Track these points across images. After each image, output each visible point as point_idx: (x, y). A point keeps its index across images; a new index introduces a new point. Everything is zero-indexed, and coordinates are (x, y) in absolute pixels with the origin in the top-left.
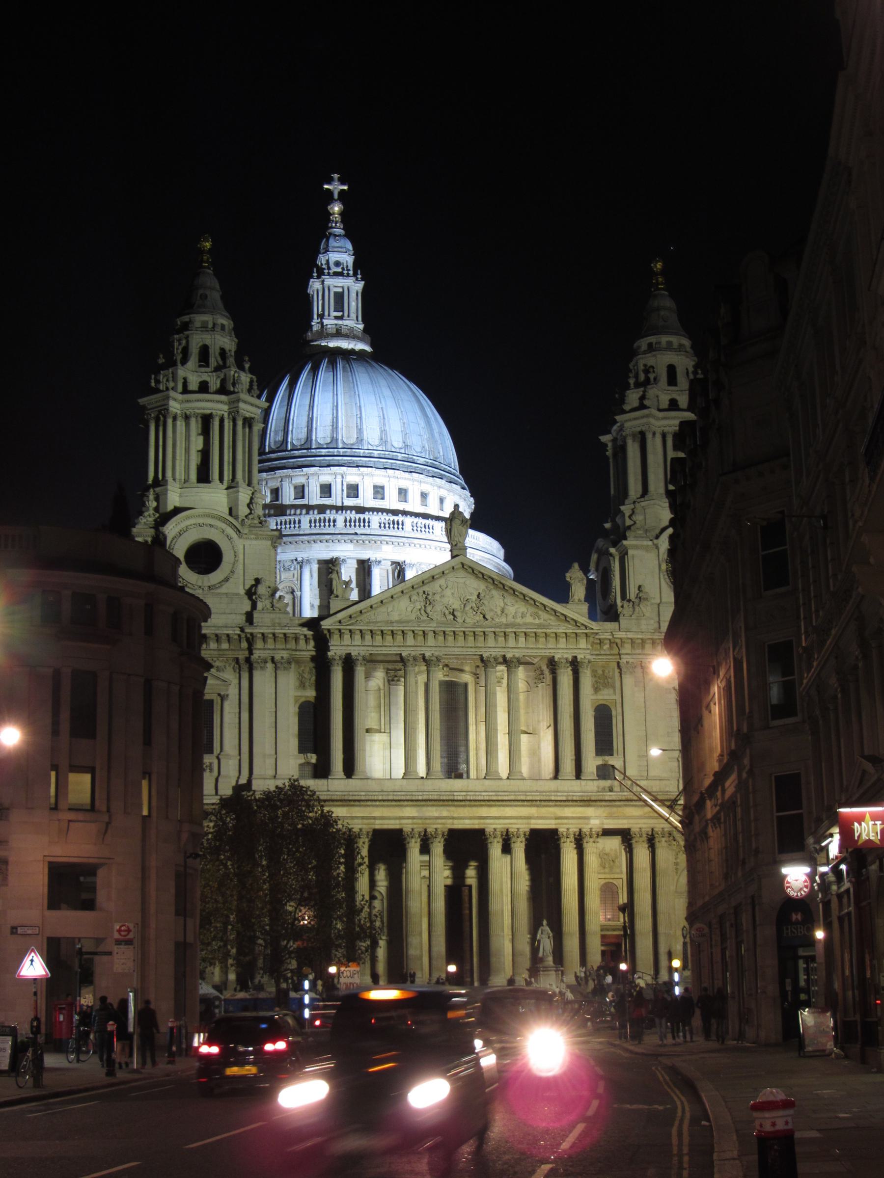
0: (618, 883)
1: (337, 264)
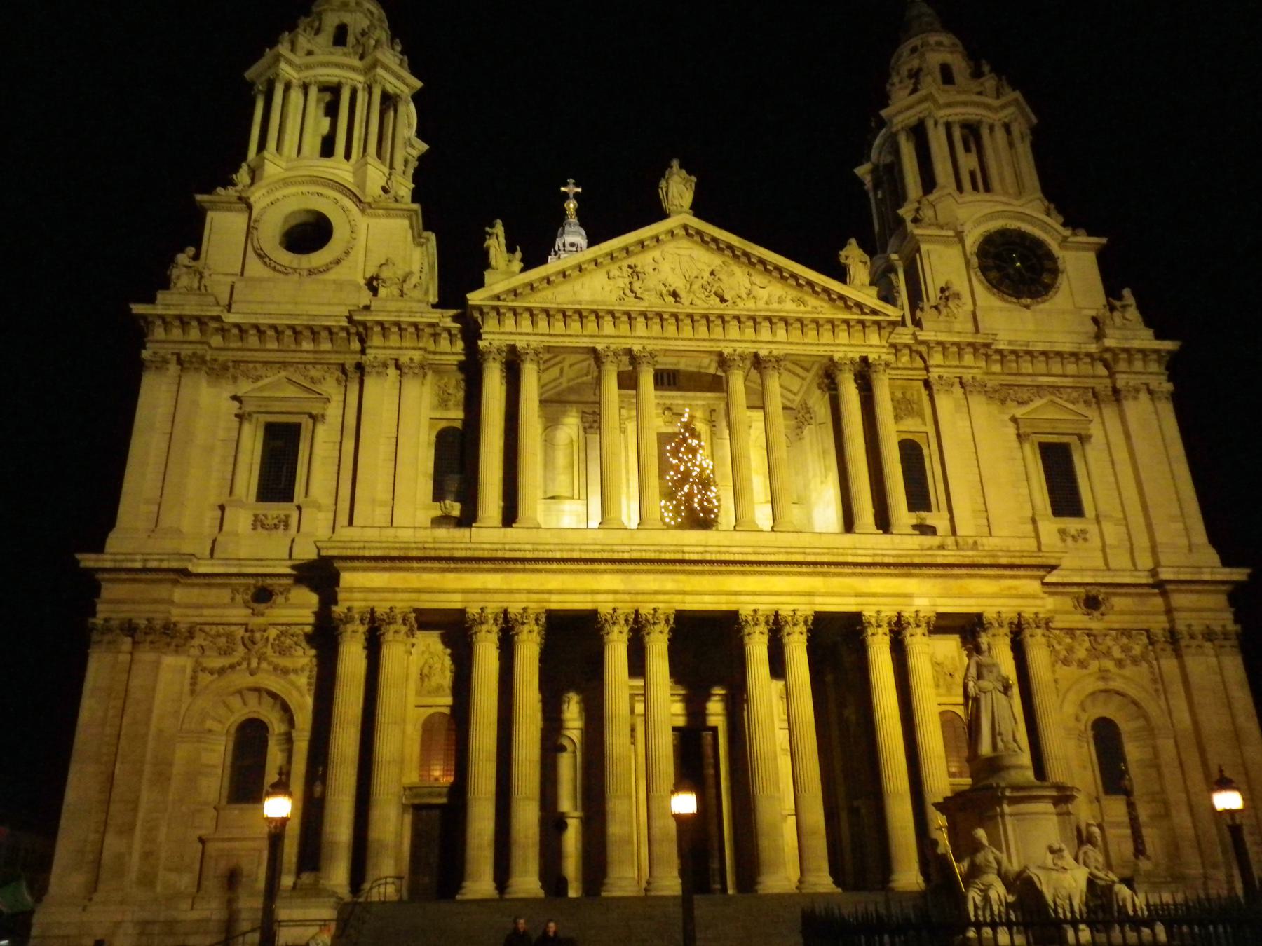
1: (572, 245)
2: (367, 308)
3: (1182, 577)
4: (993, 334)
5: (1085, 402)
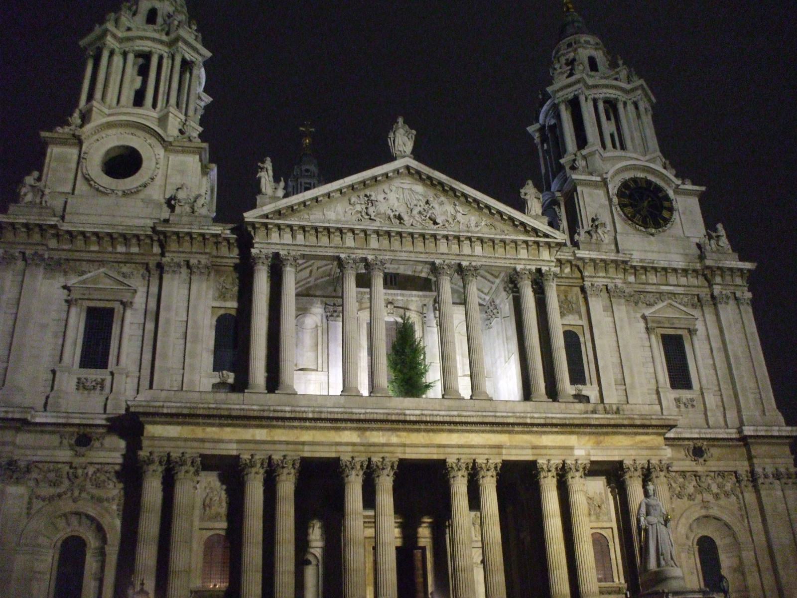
0: (607, 533)
1: (307, 171)
2: (166, 221)
3: (759, 434)
4: (630, 254)
5: (693, 305)
